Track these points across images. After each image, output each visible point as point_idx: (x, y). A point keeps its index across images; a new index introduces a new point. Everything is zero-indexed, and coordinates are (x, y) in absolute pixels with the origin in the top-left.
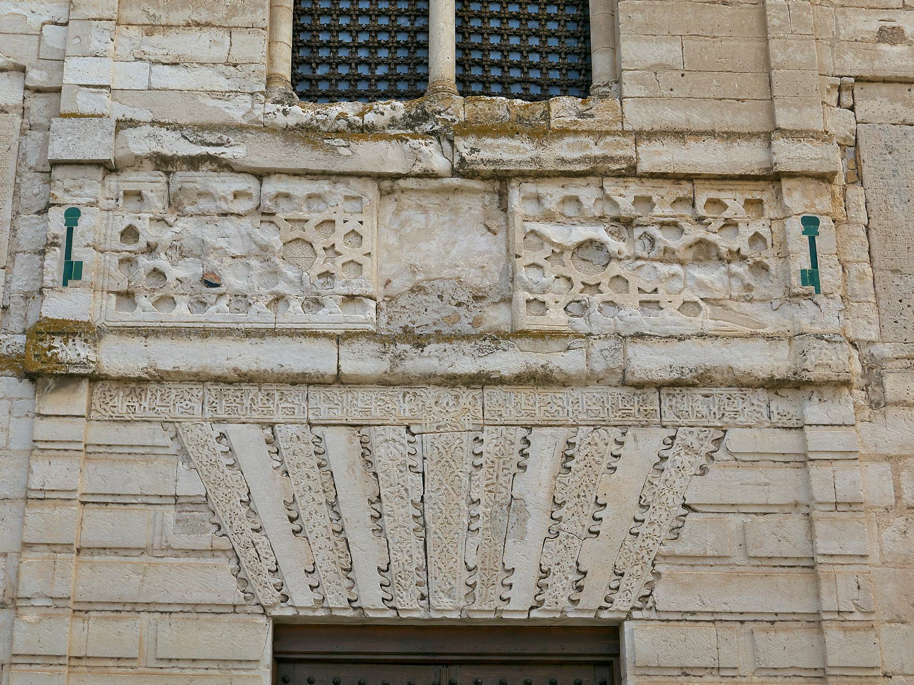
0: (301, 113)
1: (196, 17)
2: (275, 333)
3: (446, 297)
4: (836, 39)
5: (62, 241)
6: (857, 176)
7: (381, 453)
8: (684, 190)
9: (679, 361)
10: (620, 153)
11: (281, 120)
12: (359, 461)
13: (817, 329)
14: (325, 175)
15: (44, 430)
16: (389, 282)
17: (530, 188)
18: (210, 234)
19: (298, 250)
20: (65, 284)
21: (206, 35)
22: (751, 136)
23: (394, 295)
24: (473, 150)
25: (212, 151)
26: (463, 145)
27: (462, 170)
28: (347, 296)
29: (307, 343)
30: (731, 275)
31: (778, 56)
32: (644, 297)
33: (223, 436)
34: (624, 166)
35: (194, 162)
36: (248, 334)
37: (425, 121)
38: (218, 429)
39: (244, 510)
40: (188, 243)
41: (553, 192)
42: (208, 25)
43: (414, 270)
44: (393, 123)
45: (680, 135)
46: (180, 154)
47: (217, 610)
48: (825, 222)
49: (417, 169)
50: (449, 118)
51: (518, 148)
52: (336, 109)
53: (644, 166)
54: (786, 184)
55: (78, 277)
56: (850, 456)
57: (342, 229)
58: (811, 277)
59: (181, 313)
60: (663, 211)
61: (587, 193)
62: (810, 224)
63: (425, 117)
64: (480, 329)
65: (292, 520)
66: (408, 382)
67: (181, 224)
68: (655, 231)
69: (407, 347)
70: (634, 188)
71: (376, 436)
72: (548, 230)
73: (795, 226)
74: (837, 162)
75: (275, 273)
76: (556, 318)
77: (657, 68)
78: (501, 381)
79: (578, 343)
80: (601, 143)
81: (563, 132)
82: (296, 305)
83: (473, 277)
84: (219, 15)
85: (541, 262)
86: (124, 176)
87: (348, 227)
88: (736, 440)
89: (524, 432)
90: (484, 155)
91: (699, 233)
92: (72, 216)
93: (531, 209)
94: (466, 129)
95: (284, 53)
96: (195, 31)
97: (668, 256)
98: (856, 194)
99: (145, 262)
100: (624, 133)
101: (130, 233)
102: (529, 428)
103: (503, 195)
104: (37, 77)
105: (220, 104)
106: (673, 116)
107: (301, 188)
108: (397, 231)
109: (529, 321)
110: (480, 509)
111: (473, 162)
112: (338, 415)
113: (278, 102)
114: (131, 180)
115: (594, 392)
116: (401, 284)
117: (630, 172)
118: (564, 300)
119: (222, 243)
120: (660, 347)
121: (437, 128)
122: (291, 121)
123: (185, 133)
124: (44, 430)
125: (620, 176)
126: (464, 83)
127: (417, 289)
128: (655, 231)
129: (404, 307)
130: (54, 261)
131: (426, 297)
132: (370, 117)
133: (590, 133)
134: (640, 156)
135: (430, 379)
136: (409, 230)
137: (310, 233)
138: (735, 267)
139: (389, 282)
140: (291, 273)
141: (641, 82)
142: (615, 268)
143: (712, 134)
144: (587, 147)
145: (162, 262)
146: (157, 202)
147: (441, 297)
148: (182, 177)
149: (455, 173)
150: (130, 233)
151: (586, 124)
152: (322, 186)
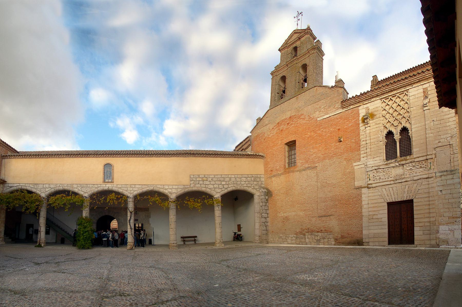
2: (385, 181)
4: (434, 144)
6: (436, 157)
7: (394, 189)
8: (419, 162)
9: (418, 178)
11: (384, 164)
13: (430, 173)
15: (369, 192)
17: (405, 165)
18: (380, 174)
22: (425, 156)
27: (399, 165)
30: (423, 169)
31: (428, 147)
35: (378, 169)
36: (383, 182)
40: (378, 175)
41: (407, 165)
43: (396, 174)
44: (394, 162)
45: (418, 157)
47: (382, 202)
52: (389, 162)
54: (428, 160)
56: (433, 183)
58: (430, 168)
59: (378, 181)
60: (417, 164)
61: (410, 164)
62: (430, 163)
63: (396, 161)
66: (396, 183)
67: (378, 174)
68: (416, 166)
70: (415, 163)
73: (429, 163)
74: (433, 156)
75: (385, 176)
76: (408, 176)
79: (409, 178)
82: (387, 179)
83: (401, 174)
88: (423, 183)
91: (420, 166)
92: (369, 175)
93: (406, 167)
94: (400, 161)
95: (385, 157)
97: (418, 168)
99: (375, 178)
101: (374, 175)
104: (365, 164)
106: (418, 156)
109: (406, 177)
112: (391, 187)
114: (373, 171)
115: (411, 181)
116: (395, 175)
117: (414, 162)
119: (381, 175)
120: (417, 177)
122: (385, 163)
124: (369, 192)
126: (401, 156)
127: (396, 175)
128: (416, 166)
132: (392, 162)
135: (397, 183)
137: (388, 173)
138: (424, 168)
140: (386, 176)
142: (413, 170)
143: (421, 157)
145: (376, 177)
146: (375, 173)
148: (377, 170)
150: (374, 175)
151: (410, 158)
152: (388, 169)
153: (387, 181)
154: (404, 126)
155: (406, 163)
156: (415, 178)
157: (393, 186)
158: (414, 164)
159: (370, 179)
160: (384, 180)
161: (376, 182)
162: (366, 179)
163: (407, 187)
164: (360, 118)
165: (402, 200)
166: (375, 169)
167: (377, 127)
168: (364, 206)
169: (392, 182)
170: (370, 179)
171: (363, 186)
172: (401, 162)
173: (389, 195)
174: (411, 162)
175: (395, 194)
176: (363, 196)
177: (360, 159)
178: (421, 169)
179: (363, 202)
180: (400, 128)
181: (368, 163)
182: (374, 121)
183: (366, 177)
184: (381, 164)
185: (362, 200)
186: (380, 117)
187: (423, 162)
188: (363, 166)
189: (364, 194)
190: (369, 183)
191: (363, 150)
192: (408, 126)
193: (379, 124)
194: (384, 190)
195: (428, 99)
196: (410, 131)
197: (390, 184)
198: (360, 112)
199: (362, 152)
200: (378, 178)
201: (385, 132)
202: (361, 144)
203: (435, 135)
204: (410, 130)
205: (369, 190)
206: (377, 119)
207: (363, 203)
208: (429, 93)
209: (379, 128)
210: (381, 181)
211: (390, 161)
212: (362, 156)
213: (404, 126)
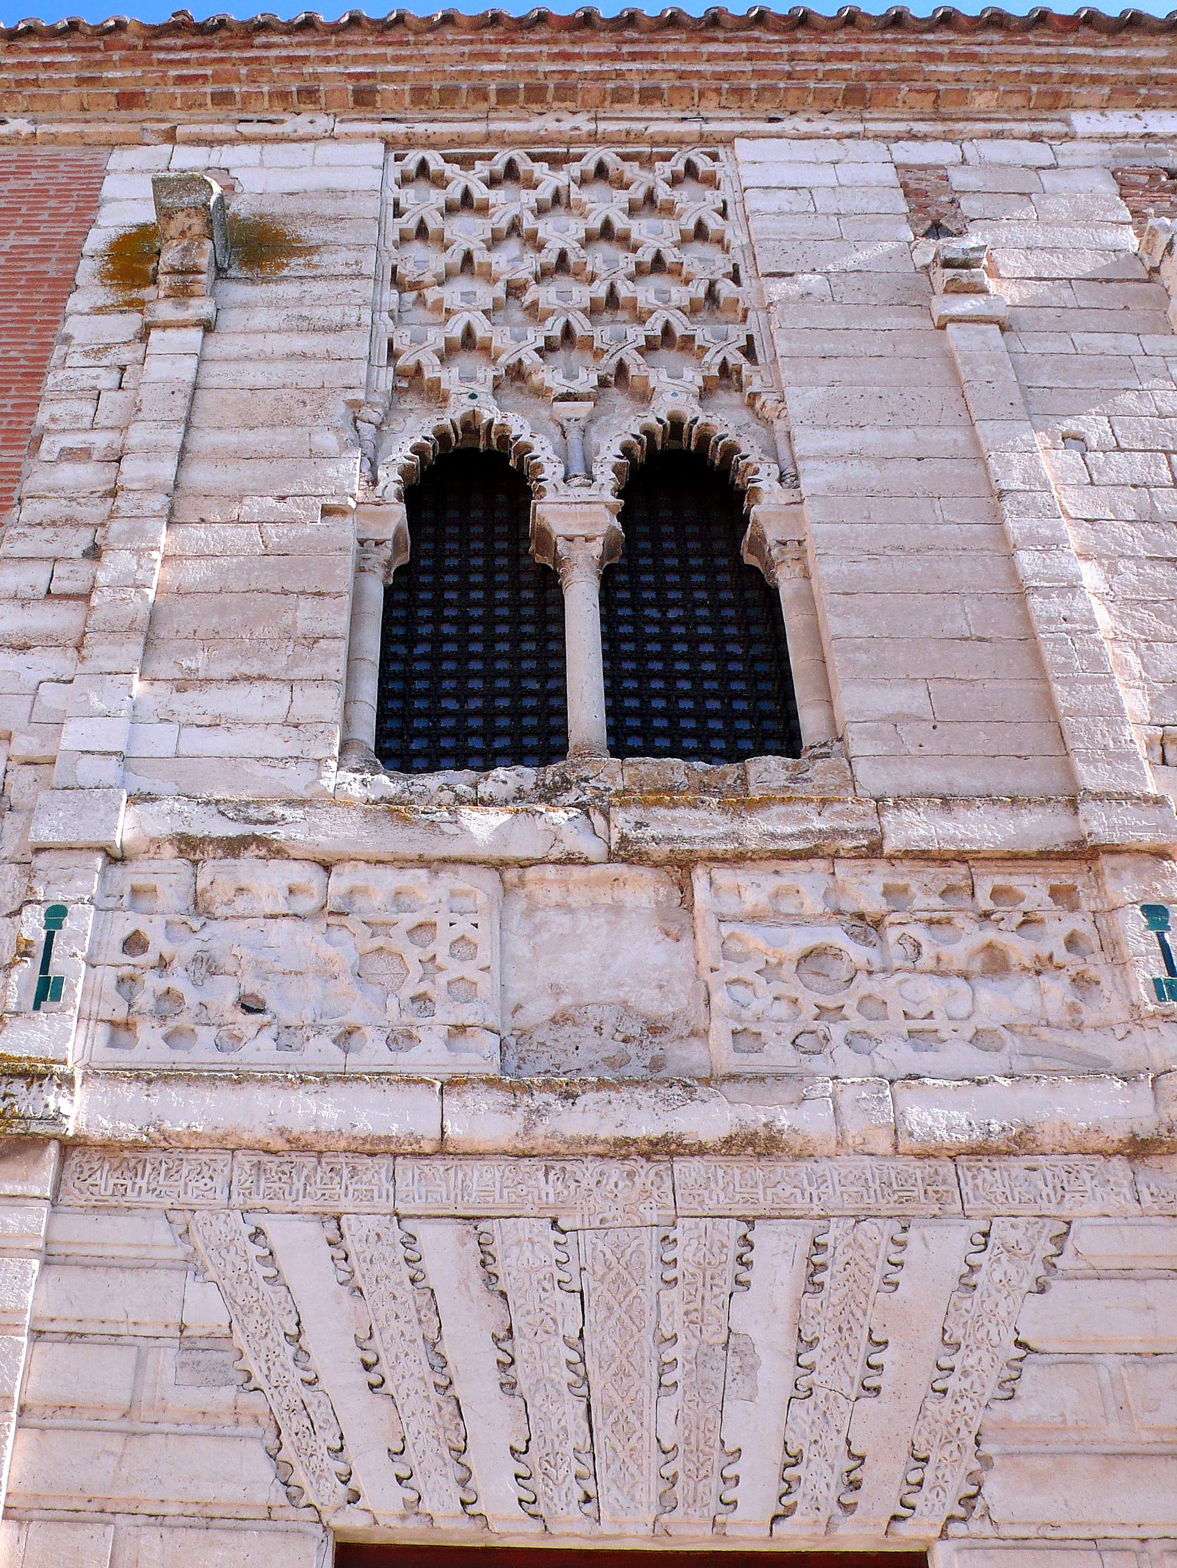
1: (245, 669)
3: (607, 1029)
12: (477, 1275)
14: (423, 862)
16: (519, 1007)
19: (379, 965)
21: (258, 691)
23: (527, 1027)
24: (639, 825)
25: (259, 830)
26: (623, 819)
28: (455, 1026)
29: (394, 1094)
33: (259, 1232)
34: (865, 842)
37: (567, 790)
39: (291, 1350)
42: (261, 678)
43: (556, 990)
46: (214, 835)
49: (555, 854)
50: (601, 786)
57: (446, 935)
63: (565, 785)
64: (663, 1074)
65: (367, 1367)
69: (550, 1097)
70: (880, 875)
77: (896, 720)
78: (701, 1151)
80: (826, 813)
83: (650, 1002)
84: (279, 664)
85: (750, 976)
86: (131, 867)
87: (456, 932)
89: (743, 1228)
96: (243, 689)
99: (153, 983)
101: (134, 943)
103: (685, 888)
105: (276, 773)
107: (390, 879)
108: (529, 937)
111: (638, 840)
113: (356, 771)
116: (538, 1010)
117: (874, 851)
118: (789, 1030)
121: (584, 798)
123: (222, 808)
129: (543, 1044)
131: (576, 1029)
134: (886, 830)
136: (546, 935)
137: (399, 941)
139: (519, 1007)
141: (875, 735)
144: (805, 818)
145: (178, 981)
147: (598, 1029)
153: (380, 1076)
157: (500, 1202)
164: (97, 240)
172: (661, 812)
182: (289, 290)
193: (341, 328)
197: (443, 1149)
198: (109, 188)
202: (29, 485)
206: (318, 288)
209: (325, 366)
211: (468, 775)
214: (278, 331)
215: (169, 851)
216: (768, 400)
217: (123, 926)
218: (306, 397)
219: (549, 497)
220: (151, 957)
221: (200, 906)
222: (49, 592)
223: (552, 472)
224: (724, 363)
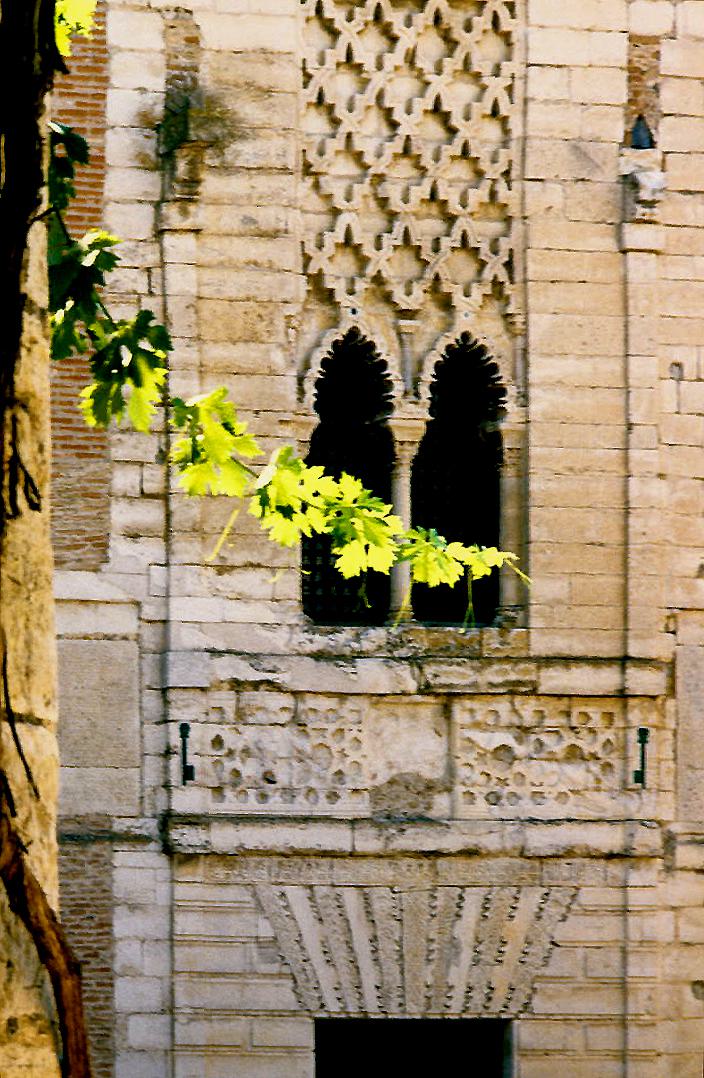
0: (320, 641)
5: (179, 750)
6: (672, 691)
7: (377, 906)
10: (527, 678)
11: (309, 648)
17: (468, 703)
20: (184, 784)
24: (436, 676)
32: (535, 789)
35: (256, 685)
38: (276, 890)
42: (259, 566)
43: (390, 765)
45: (567, 661)
48: (652, 732)
51: (463, 674)
53: (542, 690)
55: (192, 778)
57: (349, 736)
58: (640, 777)
61: (503, 706)
62: (643, 734)
68: (544, 738)
71: (375, 893)
72: (479, 737)
73: (634, 736)
81: (490, 661)
83: (428, 773)
90: (443, 680)
92: (185, 729)
98: (670, 704)
100: (529, 659)
101: (218, 742)
102: (462, 887)
104: (149, 612)
106: (561, 645)
110: (434, 946)
122: (314, 648)
125: (525, 694)
127: (392, 782)
130: (175, 762)
133: (508, 659)
135: (405, 853)
137: (329, 741)
142: (518, 767)
145: (237, 764)
148: (248, 695)
149: (420, 692)
150: (218, 742)
154: (466, 336)
155: (474, 684)
156: (540, 840)
158: (528, 709)
159: (188, 773)
160: (301, 807)
161: (231, 804)
162: (153, 765)
163: (473, 900)
165: (434, 1014)
166: (237, 685)
167: (256, 263)
168: (133, 1021)
169: (368, 841)
170: (188, 773)
171: (119, 826)
173: (341, 955)
174: (513, 690)
175: (388, 948)
176: (123, 924)
177: (102, 545)
178: (577, 773)
179: (119, 983)
180: (431, 342)
181: (179, 610)
183: (154, 737)
184: (280, 640)
185: (117, 967)
186: (285, 170)
187: (595, 712)
188: (124, 622)
189: (134, 908)
190: (187, 800)
191: (138, 455)
192: (489, 334)
194: (296, 895)
195: (655, 155)
196: (511, 405)
199: (124, 480)
200: (250, 770)
201: (317, 339)
203: (680, 494)
204: (512, 391)
205: (185, 873)
207: (125, 995)
208: (668, 99)
210: (276, 805)
212: (122, 515)
213: (466, 336)
214: (241, 235)
215: (226, 686)
216: (519, 320)
217: (213, 731)
218: (261, 311)
219: (396, 413)
220: (224, 751)
221: (241, 715)
222: (142, 492)
223: (398, 390)
224: (495, 277)
